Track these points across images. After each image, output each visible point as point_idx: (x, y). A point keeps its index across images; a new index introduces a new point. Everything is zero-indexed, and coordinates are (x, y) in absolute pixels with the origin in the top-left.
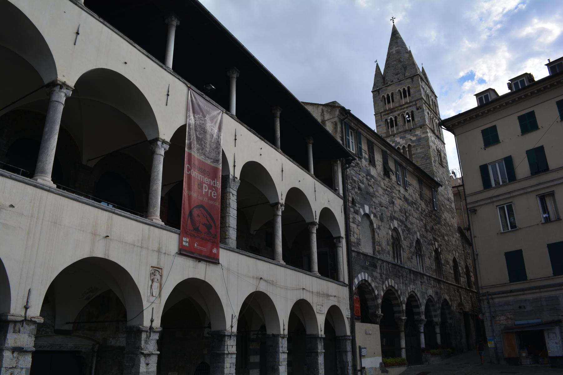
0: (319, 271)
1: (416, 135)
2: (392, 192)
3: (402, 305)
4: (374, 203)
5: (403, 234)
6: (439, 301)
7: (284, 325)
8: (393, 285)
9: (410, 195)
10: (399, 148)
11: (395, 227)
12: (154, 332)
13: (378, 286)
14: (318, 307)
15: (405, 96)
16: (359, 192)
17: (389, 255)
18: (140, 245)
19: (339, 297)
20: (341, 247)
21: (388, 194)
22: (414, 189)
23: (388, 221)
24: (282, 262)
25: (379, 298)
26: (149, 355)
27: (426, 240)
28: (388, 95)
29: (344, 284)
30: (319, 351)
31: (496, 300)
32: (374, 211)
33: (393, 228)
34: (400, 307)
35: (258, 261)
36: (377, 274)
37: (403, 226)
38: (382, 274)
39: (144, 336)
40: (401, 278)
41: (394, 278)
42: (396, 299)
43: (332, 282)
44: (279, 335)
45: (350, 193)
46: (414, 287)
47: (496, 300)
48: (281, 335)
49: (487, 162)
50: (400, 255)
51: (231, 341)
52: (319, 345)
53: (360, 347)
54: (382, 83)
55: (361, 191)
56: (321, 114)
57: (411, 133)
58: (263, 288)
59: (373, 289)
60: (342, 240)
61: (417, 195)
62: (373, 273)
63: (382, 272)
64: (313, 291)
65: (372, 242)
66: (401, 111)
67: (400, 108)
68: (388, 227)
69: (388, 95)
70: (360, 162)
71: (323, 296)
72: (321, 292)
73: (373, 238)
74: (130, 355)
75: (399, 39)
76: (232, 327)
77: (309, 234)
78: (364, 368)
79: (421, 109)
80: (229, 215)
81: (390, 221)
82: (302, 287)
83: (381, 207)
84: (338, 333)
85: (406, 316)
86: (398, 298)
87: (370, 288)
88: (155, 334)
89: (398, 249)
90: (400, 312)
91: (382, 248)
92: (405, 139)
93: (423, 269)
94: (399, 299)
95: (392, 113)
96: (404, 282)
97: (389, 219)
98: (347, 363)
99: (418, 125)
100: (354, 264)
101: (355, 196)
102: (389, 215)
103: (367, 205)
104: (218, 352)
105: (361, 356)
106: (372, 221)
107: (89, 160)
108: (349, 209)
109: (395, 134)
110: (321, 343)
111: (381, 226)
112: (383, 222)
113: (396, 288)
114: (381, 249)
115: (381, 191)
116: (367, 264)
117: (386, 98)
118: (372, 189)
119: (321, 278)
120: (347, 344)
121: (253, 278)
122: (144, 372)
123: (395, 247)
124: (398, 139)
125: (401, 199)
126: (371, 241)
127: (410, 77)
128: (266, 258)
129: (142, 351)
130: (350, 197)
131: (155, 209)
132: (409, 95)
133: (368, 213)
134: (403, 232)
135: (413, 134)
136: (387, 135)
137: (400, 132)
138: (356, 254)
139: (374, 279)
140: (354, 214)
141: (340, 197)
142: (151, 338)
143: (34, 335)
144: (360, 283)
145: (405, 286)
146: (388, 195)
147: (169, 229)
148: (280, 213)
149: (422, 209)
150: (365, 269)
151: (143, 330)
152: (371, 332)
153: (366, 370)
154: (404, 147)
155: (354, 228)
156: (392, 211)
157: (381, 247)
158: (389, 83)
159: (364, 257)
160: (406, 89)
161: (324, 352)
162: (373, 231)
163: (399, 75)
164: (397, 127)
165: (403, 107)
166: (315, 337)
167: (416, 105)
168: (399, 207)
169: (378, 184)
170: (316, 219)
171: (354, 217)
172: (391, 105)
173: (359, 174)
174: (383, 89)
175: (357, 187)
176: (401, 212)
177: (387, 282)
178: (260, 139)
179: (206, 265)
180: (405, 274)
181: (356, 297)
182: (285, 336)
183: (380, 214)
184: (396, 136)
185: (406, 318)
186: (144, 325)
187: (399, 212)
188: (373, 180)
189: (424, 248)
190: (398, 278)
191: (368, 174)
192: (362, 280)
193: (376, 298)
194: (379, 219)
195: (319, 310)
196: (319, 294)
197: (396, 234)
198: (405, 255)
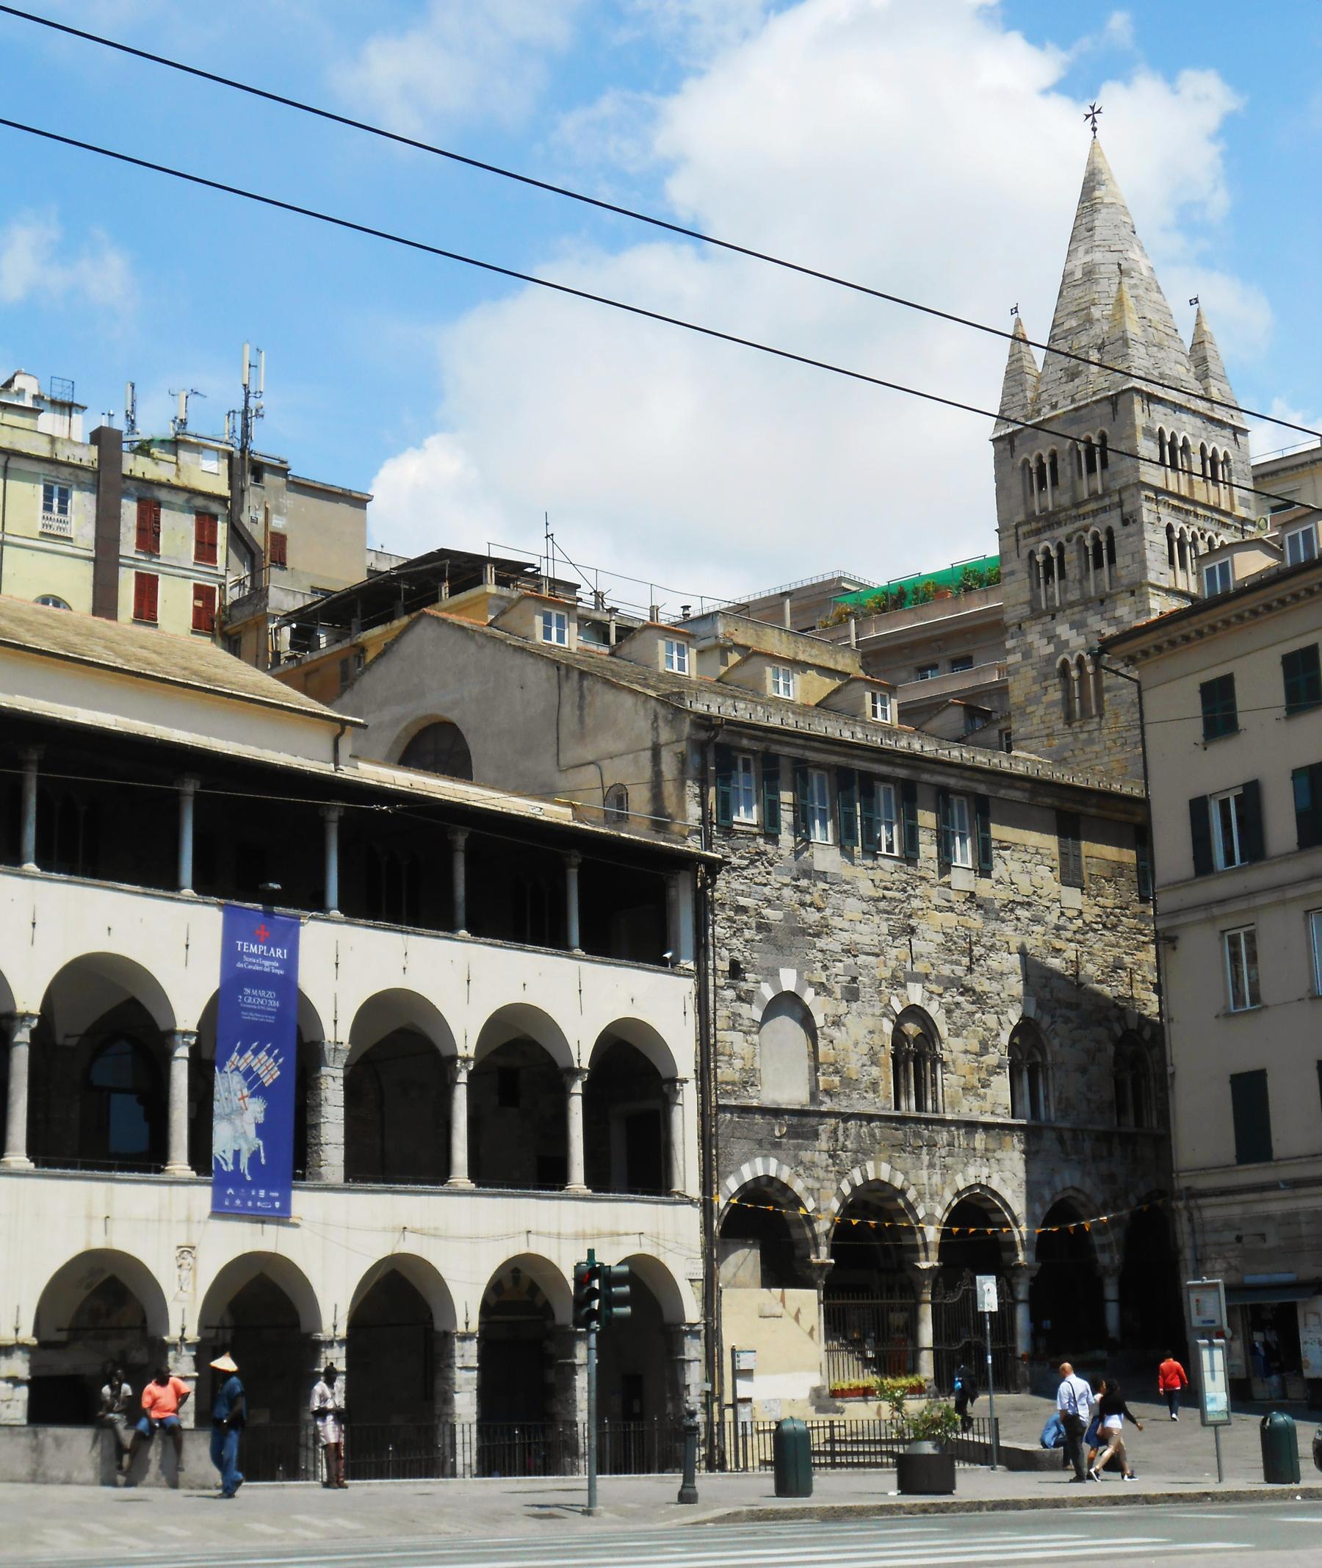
1: (1116, 621)
4: (820, 955)
10: (1065, 663)
13: (817, 1185)
15: (1091, 469)
22: (1027, 857)
24: (467, 1184)
27: (1072, 1014)
28: (1040, 458)
31: (1208, 1214)
32: (821, 976)
36: (818, 1153)
39: (171, 1354)
41: (890, 1157)
46: (985, 1171)
47: (1208, 1214)
50: (934, 1084)
56: (653, 724)
57: (1102, 608)
58: (410, 1246)
61: (1044, 871)
62: (802, 1153)
64: (562, 1232)
67: (1073, 512)
68: (878, 1011)
69: (1040, 458)
70: (769, 848)
73: (814, 1053)
75: (1104, 211)
76: (335, 1327)
77: (564, 1095)
78: (747, 1401)
79: (1134, 521)
92: (1085, 630)
93: (1047, 1107)
95: (1049, 526)
96: (938, 1162)
99: (1125, 581)
107: (67, 1036)
109: (1058, 610)
115: (853, 907)
124: (1064, 631)
125: (951, 909)
126: (805, 1063)
127: (1107, 398)
134: (949, 1012)
135: (1107, 615)
136: (1033, 610)
137: (1071, 605)
139: (801, 1171)
140: (738, 1003)
148: (463, 1077)
149: (1062, 914)
154: (1080, 658)
164: (1062, 581)
165: (1082, 511)
168: (941, 938)
169: (845, 892)
171: (733, 1014)
172: (1048, 499)
173: (765, 885)
175: (754, 925)
178: (402, 932)
184: (1059, 616)
187: (934, 955)
188: (821, 885)
189: (1056, 1042)
198: (949, 1082)
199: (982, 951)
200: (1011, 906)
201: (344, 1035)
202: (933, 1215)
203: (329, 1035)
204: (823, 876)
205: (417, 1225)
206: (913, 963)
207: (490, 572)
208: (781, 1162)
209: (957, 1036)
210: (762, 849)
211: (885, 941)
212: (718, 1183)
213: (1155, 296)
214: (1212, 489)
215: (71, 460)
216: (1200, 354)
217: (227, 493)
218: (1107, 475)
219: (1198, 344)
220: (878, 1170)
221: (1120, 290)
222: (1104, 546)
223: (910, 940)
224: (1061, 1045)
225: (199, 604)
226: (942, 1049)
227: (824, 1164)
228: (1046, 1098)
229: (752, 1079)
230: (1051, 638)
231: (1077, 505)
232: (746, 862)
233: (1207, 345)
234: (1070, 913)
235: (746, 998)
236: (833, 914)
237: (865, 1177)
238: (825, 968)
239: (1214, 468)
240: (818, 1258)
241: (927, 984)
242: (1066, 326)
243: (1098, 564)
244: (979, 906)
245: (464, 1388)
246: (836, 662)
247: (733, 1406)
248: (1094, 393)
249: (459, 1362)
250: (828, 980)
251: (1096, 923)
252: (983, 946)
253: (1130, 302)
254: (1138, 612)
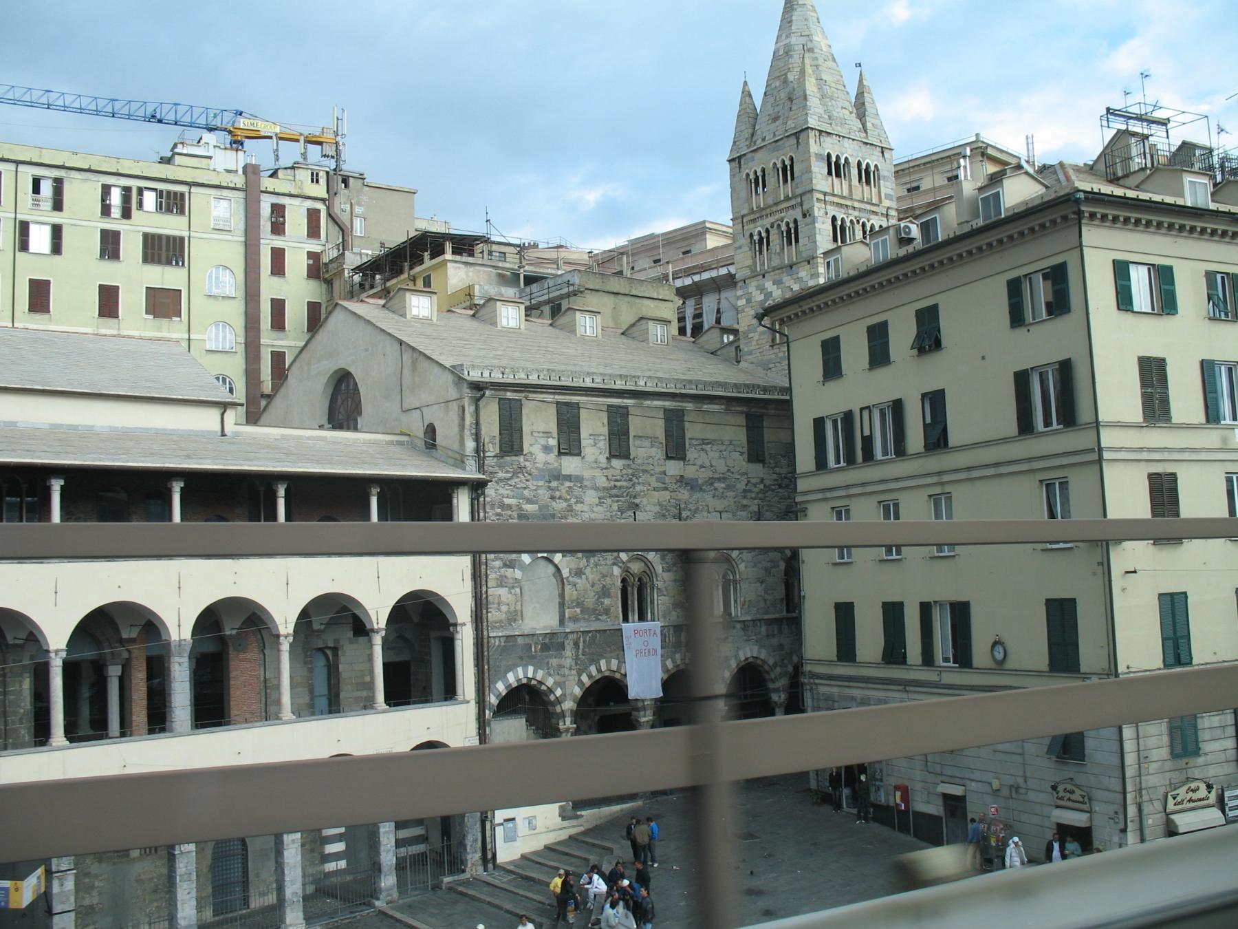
1: (799, 280)
2: (633, 485)
6: (785, 661)
9: (702, 467)
13: (563, 679)
22: (724, 447)
28: (756, 172)
31: (822, 689)
49: (824, 415)
50: (652, 602)
54: (747, 139)
61: (736, 455)
66: (778, 216)
67: (774, 209)
70: (527, 464)
73: (562, 595)
87: (543, 687)
92: (782, 286)
93: (736, 607)
99: (804, 255)
117: (753, 181)
124: (769, 286)
125: (666, 489)
132: (793, 178)
135: (795, 277)
137: (775, 269)
146: (618, 496)
149: (748, 481)
158: (759, 143)
160: (787, 162)
163: (777, 123)
167: (802, 205)
168: (657, 509)
171: (501, 576)
173: (525, 488)
174: (747, 156)
184: (766, 275)
188: (567, 484)
189: (742, 566)
191: (557, 476)
197: (643, 564)
199: (689, 513)
200: (711, 482)
201: (187, 634)
203: (174, 636)
204: (569, 478)
207: (448, 247)
210: (522, 465)
211: (616, 515)
212: (489, 687)
213: (831, 64)
214: (866, 188)
215: (230, 185)
216: (861, 101)
217: (325, 196)
218: (794, 184)
219: (860, 95)
221: (803, 62)
222: (793, 231)
223: (634, 513)
224: (746, 567)
225: (311, 262)
226: (657, 580)
228: (736, 602)
230: (762, 289)
231: (776, 204)
232: (510, 475)
233: (865, 94)
234: (753, 481)
236: (577, 502)
239: (867, 175)
240: (565, 724)
242: (773, 86)
243: (790, 243)
244: (687, 484)
245: (291, 846)
246: (658, 293)
248: (786, 131)
251: (774, 485)
252: (690, 510)
253: (809, 70)
254: (812, 275)
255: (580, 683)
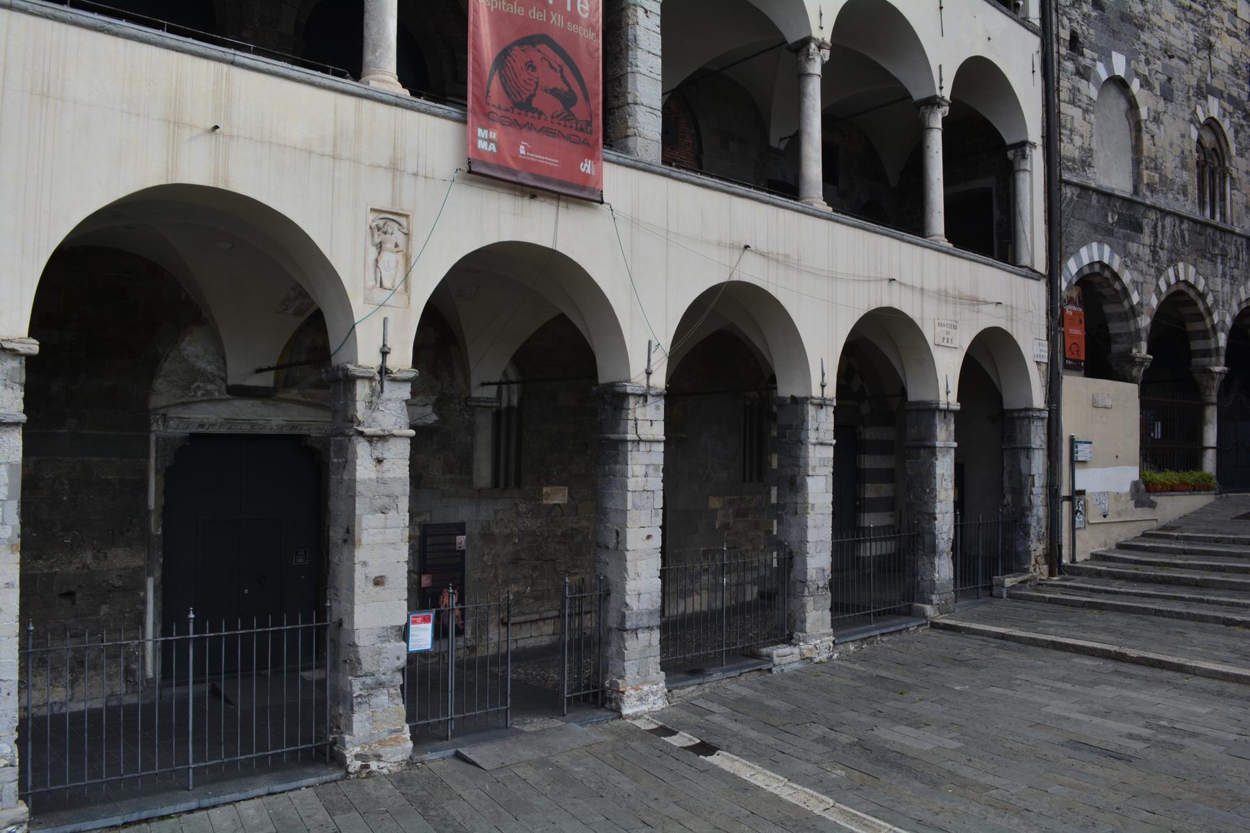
0: (949, 235)
2: (1207, 16)
3: (1215, 333)
5: (1236, 137)
7: (823, 375)
8: (1191, 280)
11: (1213, 118)
12: (394, 380)
13: (1141, 279)
14: (939, 329)
16: (1094, 14)
17: (1185, 195)
18: (328, 150)
19: (1012, 307)
20: (1026, 170)
21: (1195, 19)
23: (1189, 99)
25: (1142, 313)
26: (383, 438)
29: (1032, 273)
30: (938, 444)
32: (1143, 69)
33: (1202, 119)
34: (1209, 338)
35: (735, 200)
36: (1141, 247)
37: (1239, 114)
38: (1158, 249)
39: (362, 390)
40: (1219, 261)
41: (1195, 260)
42: (1199, 317)
43: (991, 265)
44: (807, 399)
45: (1065, 17)
48: (812, 397)
50: (1223, 198)
51: (647, 408)
52: (938, 430)
53: (1072, 441)
55: (1103, 10)
58: (752, 272)
59: (1125, 289)
60: (1031, 151)
62: (1130, 244)
63: (1158, 244)
64: (926, 287)
65: (1132, 159)
68: (1188, 117)
71: (958, 300)
72: (951, 291)
73: (1137, 148)
74: (339, 438)
76: (649, 373)
77: (922, 131)
78: (1082, 493)
80: (635, 69)
81: (1194, 99)
82: (886, 276)
83: (1167, 58)
84: (1011, 401)
85: (1225, 366)
86: (1205, 315)
87: (1117, 286)
88: (396, 385)
89: (1218, 180)
90: (1207, 353)
91: (1164, 180)
94: (1208, 320)
96: (1228, 272)
97: (1191, 94)
98: (1030, 479)
100: (1069, 220)
101: (1081, 25)
102: (1194, 82)
103: (1120, 51)
104: (613, 436)
105: (1073, 462)
106: (1135, 100)
108: (1059, 63)
110: (948, 425)
111: (1165, 112)
112: (1172, 101)
113: (1201, 287)
114: (1160, 178)
116: (1110, 220)
118: (1141, 6)
119: (952, 251)
120: (1033, 429)
121: (719, 245)
122: (370, 479)
123: (1207, 176)
125: (1237, 36)
126: (1128, 157)
128: (764, 193)
129: (360, 429)
130: (1063, 28)
131: (377, 54)
133: (1123, 76)
134: (1236, 132)
138: (1076, 191)
139: (1129, 263)
140: (1077, 78)
141: (1028, 29)
142: (386, 395)
143: (20, 384)
144: (1086, 271)
145: (1231, 284)
146: (1193, 22)
147: (424, 106)
148: (816, 68)
150: (1104, 233)
151: (357, 374)
152: (1109, 403)
153: (1087, 497)
155: (1073, 118)
156: (1205, 69)
157: (1160, 174)
159: (1102, 201)
161: (955, 448)
162: (1137, 127)
166: (930, 410)
168: (1230, 61)
170: (941, 88)
171: (1073, 86)
176: (1237, 74)
177: (1171, 271)
179: (558, 207)
180: (1234, 249)
181: (1073, 311)
182: (828, 402)
183: (1163, 78)
185: (1226, 369)
186: (359, 363)
190: (1211, 260)
192: (1091, 264)
193: (1134, 312)
194: (1159, 94)
195: (944, 339)
196: (946, 296)
197: (1214, 138)
202: (1224, 322)
205: (763, 248)
206: (1212, 77)
208: (1113, 250)
209: (1242, 156)
212: (1060, 262)
220: (1187, 271)
227: (1147, 260)
229: (1090, 159)
235: (1084, 73)
237: (1177, 277)
238: (1148, 62)
241: (1222, 101)
245: (819, 471)
247: (1070, 498)
249: (812, 436)
250: (1150, 75)
255: (1158, 290)
